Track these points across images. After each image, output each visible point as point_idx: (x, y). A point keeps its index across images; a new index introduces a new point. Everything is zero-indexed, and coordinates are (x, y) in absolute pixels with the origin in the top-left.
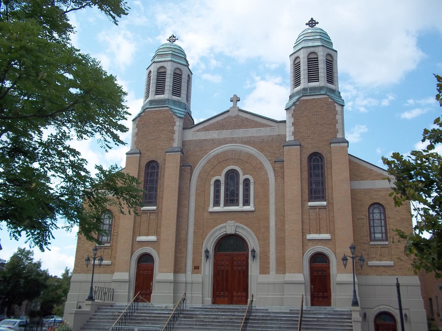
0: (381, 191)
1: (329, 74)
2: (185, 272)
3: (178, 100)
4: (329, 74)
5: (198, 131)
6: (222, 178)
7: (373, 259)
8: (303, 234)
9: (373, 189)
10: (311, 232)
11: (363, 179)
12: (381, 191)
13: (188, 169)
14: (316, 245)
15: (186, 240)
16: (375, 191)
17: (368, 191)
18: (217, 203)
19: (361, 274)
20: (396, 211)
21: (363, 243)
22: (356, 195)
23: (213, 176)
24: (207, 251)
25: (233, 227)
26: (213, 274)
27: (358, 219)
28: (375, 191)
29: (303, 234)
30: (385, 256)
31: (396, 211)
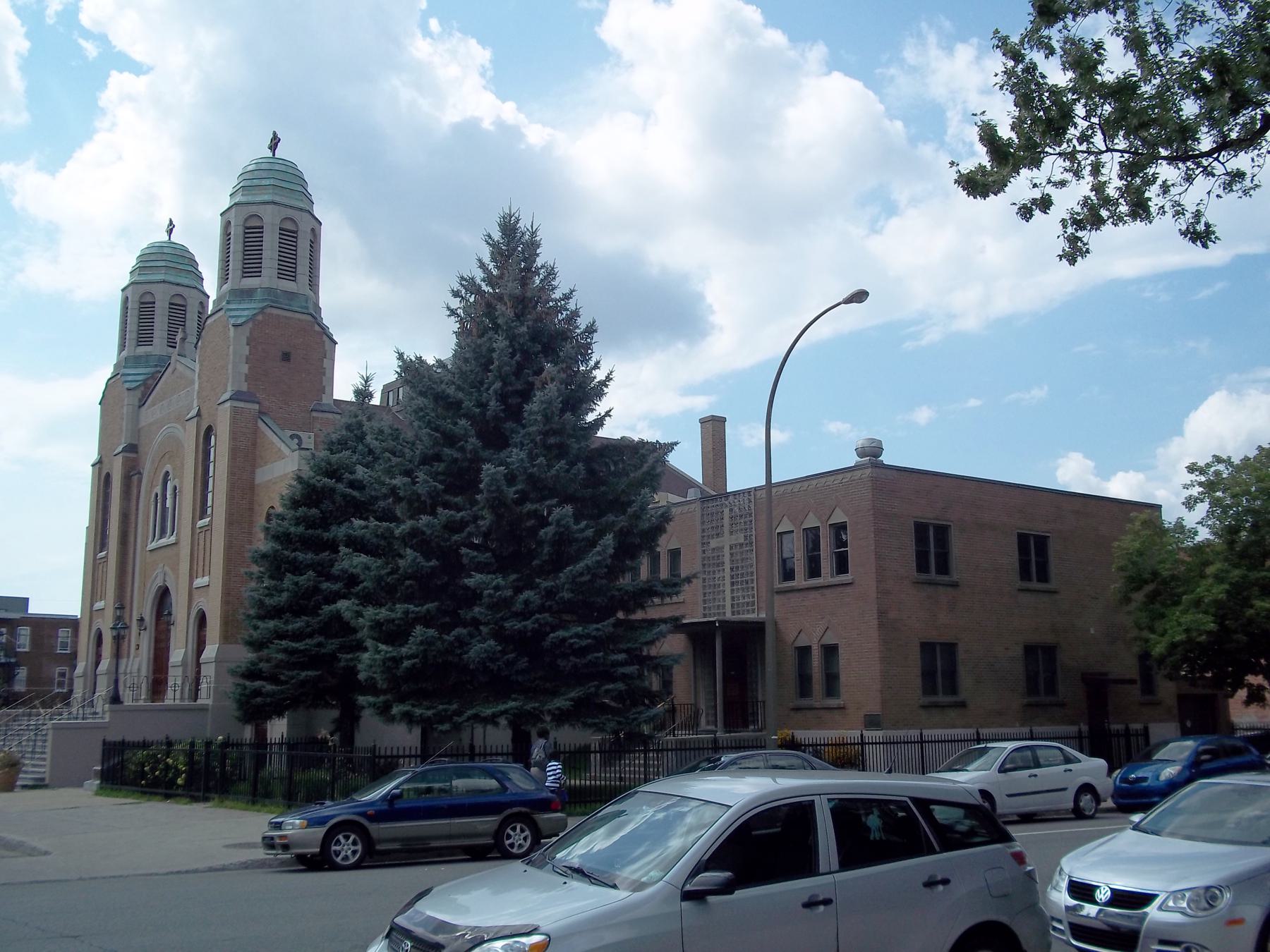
2: (128, 657)
5: (149, 407)
6: (158, 489)
13: (135, 478)
16: (274, 483)
24: (141, 620)
26: (152, 656)
28: (274, 483)
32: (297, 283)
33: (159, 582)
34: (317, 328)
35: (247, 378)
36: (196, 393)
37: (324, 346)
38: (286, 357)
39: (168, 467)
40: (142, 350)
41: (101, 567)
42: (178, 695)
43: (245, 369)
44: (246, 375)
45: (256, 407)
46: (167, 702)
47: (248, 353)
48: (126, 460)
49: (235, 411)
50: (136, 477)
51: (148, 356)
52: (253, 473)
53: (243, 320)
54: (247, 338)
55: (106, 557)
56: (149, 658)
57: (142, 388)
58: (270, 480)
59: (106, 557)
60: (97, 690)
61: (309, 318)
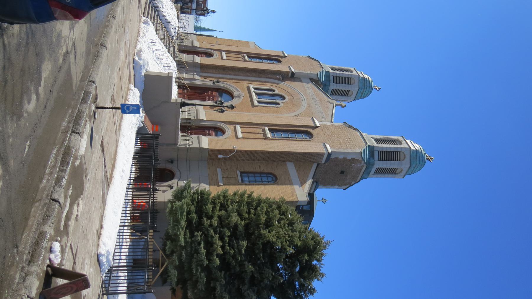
1: (388, 170)
3: (331, 80)
4: (388, 170)
6: (276, 92)
7: (224, 171)
8: (240, 123)
9: (290, 177)
10: (242, 128)
11: (298, 171)
14: (231, 129)
15: (225, 74)
16: (288, 177)
17: (287, 173)
18: (255, 89)
19: (209, 164)
21: (238, 167)
23: (278, 89)
25: (239, 95)
26: (201, 86)
27: (259, 165)
28: (288, 177)
29: (240, 123)
30: (227, 180)
31: (272, 190)
32: (373, 174)
33: (235, 93)
34: (353, 183)
35: (336, 159)
36: (325, 123)
38: (342, 172)
39: (287, 99)
40: (331, 78)
41: (241, 56)
42: (184, 117)
43: (341, 157)
44: (338, 158)
45: (323, 162)
46: (180, 134)
47: (347, 158)
48: (287, 73)
49: (323, 154)
50: (281, 78)
51: (329, 81)
52: (291, 161)
54: (354, 158)
55: (245, 61)
56: (200, 85)
57: (317, 80)
58: (289, 175)
59: (245, 61)
60: (188, 75)
61: (357, 181)
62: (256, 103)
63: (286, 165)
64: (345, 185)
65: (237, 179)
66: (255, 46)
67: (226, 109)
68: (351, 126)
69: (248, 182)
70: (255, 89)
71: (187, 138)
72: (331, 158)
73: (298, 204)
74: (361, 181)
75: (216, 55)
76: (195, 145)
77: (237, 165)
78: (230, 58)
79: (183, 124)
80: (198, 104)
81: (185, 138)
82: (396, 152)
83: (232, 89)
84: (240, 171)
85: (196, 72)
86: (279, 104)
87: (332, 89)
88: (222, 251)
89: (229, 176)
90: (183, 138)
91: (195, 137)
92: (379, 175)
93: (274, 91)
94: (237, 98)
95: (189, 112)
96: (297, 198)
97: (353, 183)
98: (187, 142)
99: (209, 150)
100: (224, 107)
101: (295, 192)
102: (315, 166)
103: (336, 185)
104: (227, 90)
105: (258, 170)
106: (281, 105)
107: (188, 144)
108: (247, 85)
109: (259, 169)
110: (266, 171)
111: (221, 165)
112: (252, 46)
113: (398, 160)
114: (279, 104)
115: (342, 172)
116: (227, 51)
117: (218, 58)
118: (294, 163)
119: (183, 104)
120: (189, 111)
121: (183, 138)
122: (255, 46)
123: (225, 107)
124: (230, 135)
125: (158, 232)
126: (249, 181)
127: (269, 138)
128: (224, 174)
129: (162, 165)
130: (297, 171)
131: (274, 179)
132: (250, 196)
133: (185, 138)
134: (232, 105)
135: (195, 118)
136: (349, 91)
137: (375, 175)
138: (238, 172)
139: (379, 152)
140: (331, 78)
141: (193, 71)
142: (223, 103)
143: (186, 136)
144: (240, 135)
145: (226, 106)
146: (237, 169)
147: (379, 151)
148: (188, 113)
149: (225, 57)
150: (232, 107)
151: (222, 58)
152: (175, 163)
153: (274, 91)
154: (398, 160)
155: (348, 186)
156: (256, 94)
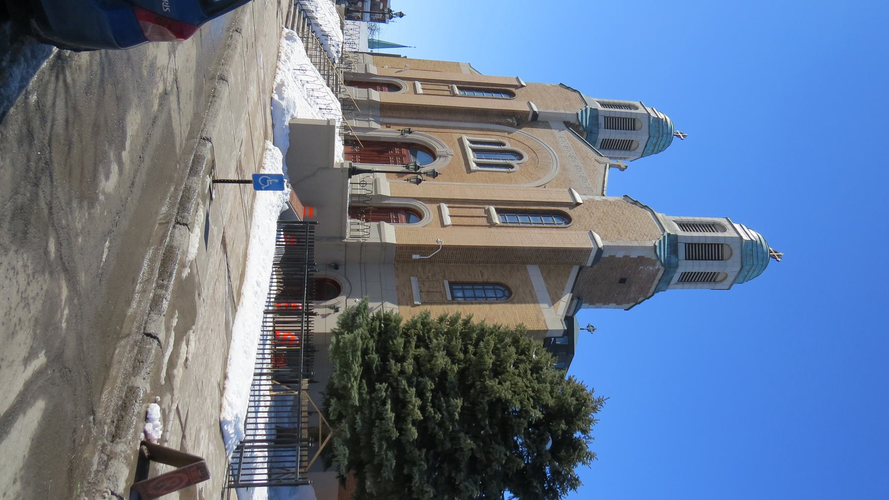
0: (533, 297)
6: (508, 147)
7: (421, 282)
10: (451, 209)
12: (533, 297)
14: (433, 211)
15: (422, 119)
16: (530, 291)
17: (527, 282)
18: (472, 142)
19: (397, 270)
20: (503, 313)
21: (445, 274)
22: (518, 270)
23: (510, 142)
25: (446, 153)
26: (382, 140)
27: (481, 271)
30: (428, 296)
31: (503, 313)
32: (676, 284)
33: (439, 150)
34: (641, 299)
35: (612, 258)
36: (591, 197)
37: (626, 303)
38: (623, 281)
39: (526, 158)
40: (601, 121)
41: (446, 88)
42: (355, 192)
43: (620, 255)
44: (615, 256)
45: (589, 264)
46: (349, 221)
47: (631, 257)
48: (527, 113)
49: (589, 250)
51: (597, 125)
52: (534, 263)
53: (658, 253)
54: (643, 257)
55: (454, 95)
56: (380, 138)
57: (577, 123)
59: (454, 95)
61: (649, 295)
62: (474, 166)
63: (526, 269)
64: (628, 302)
65: (444, 295)
66: (470, 70)
67: (424, 177)
68: (637, 201)
69: (462, 299)
70: (472, 142)
71: (361, 227)
72: (603, 256)
73: (548, 335)
74: (656, 295)
75: (406, 86)
76: (374, 238)
77: (444, 271)
78: (429, 92)
79: (353, 204)
80: (377, 170)
81: (357, 227)
82: (716, 245)
83: (433, 144)
84: (450, 280)
85: (373, 116)
86: (512, 167)
87: (603, 139)
88: (421, 415)
89: (431, 290)
90: (354, 227)
91: (374, 225)
92: (687, 285)
93: (504, 145)
94: (442, 159)
95: (363, 184)
96: (546, 326)
97: (641, 299)
98: (361, 233)
99: (396, 247)
100: (420, 173)
101: (542, 315)
102: (575, 269)
103: (611, 303)
104: (425, 145)
105: (480, 280)
106: (517, 168)
107: (363, 237)
108: (458, 136)
109: (481, 276)
110: (492, 280)
111: (418, 271)
112: (465, 71)
113: (720, 258)
114: (512, 167)
115: (623, 281)
116: (423, 81)
117: (408, 93)
118: (539, 266)
119: (353, 171)
120: (362, 182)
121: (354, 227)
122: (470, 70)
123: (423, 175)
124: (431, 220)
125: (316, 382)
126: (464, 297)
127: (497, 224)
128: (422, 285)
129: (321, 273)
130: (545, 279)
131: (507, 293)
132: (466, 322)
133: (357, 227)
134: (434, 171)
135: (374, 194)
136: (632, 141)
137: (681, 285)
138: (446, 283)
139: (687, 245)
140: (601, 121)
141: (368, 116)
142: (419, 167)
143: (358, 224)
144: (448, 221)
145: (424, 173)
146: (444, 277)
147: (686, 244)
148: (362, 185)
149: (420, 91)
150: (434, 174)
151: (416, 93)
152: (341, 269)
153: (504, 145)
154: (720, 258)
155: (632, 304)
156: (474, 150)
